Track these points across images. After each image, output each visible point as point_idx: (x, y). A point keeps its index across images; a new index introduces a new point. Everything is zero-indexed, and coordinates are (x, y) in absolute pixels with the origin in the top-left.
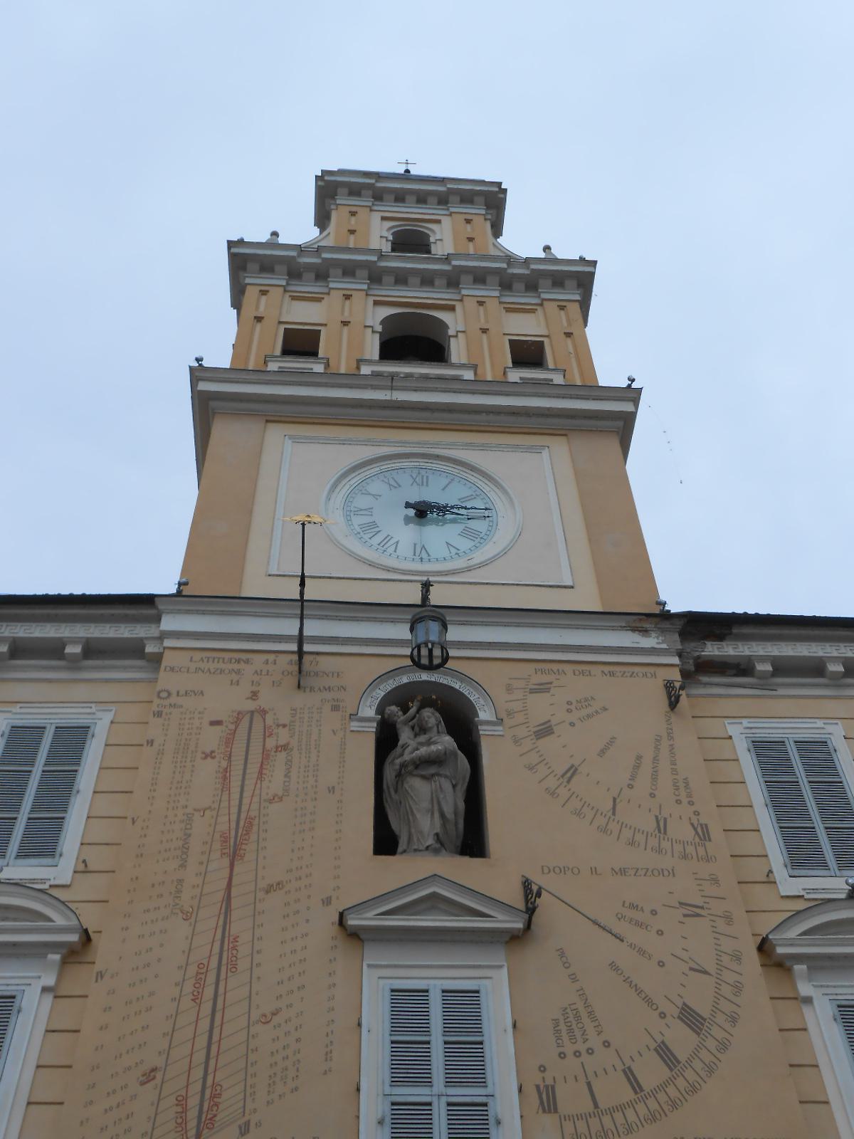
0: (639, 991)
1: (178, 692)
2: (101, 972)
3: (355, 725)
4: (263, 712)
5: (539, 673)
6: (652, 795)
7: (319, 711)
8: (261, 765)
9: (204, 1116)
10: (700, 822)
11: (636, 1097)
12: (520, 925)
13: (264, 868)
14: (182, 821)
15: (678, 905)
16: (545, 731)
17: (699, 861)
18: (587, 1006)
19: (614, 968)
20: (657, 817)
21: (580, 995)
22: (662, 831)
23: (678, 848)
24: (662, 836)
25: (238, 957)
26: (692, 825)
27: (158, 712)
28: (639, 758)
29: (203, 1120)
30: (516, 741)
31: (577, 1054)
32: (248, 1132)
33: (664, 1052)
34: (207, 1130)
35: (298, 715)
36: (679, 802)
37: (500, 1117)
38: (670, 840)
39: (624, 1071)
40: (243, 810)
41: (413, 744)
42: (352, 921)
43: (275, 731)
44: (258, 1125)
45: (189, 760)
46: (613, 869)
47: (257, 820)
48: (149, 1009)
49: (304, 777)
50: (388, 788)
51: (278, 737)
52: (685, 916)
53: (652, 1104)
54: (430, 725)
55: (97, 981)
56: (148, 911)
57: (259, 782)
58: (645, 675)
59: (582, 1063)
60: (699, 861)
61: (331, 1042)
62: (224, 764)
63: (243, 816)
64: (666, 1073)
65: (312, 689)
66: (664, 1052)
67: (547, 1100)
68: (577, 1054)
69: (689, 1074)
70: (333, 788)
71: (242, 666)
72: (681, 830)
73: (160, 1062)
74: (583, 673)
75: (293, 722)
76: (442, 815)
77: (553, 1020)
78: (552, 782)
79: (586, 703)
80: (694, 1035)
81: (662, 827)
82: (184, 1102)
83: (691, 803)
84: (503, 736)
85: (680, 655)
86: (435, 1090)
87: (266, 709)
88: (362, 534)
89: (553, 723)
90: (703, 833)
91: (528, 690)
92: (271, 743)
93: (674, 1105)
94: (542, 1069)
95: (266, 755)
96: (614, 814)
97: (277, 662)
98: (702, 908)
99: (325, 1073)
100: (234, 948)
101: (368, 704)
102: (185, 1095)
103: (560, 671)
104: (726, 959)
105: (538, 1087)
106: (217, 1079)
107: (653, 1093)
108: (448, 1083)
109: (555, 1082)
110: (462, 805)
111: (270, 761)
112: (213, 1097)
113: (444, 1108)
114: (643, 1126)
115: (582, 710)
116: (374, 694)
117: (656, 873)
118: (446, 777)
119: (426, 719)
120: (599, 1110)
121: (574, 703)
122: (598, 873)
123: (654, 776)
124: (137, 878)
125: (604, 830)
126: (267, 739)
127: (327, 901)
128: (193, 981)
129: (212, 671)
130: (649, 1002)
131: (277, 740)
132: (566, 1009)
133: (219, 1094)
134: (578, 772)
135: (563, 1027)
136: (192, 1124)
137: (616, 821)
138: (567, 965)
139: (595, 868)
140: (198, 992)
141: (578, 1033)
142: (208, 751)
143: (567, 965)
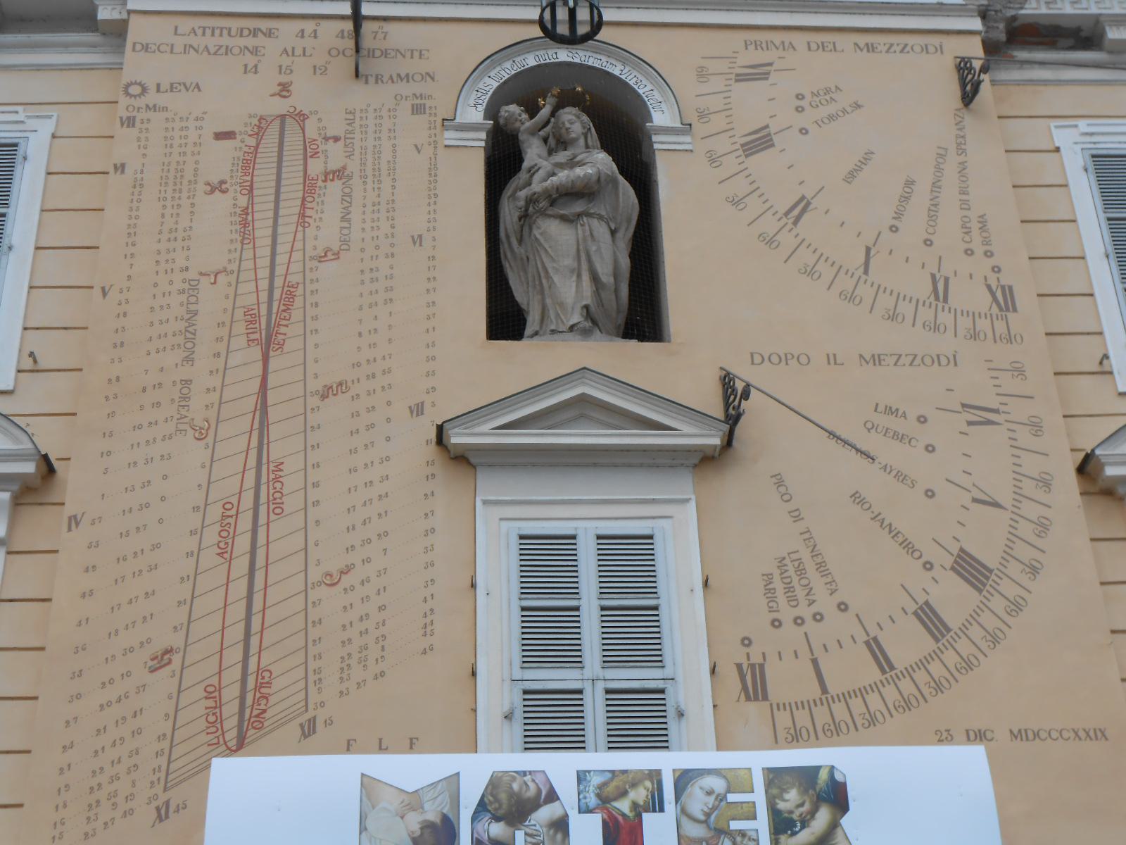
0: (894, 533)
1: (158, 86)
2: (75, 517)
3: (450, 137)
4: (301, 117)
6: (928, 243)
7: (392, 113)
9: (248, 712)
10: (1003, 283)
11: (883, 678)
12: (716, 441)
13: (316, 361)
14: (182, 292)
15: (960, 409)
16: (760, 142)
19: (857, 500)
20: (933, 276)
21: (804, 540)
23: (964, 323)
24: (940, 305)
25: (285, 491)
26: (989, 287)
27: (128, 118)
28: (910, 183)
29: (247, 716)
30: (713, 159)
31: (799, 621)
32: (314, 732)
34: (253, 731)
35: (358, 122)
36: (969, 252)
37: (683, 707)
38: (953, 311)
39: (867, 643)
40: (277, 273)
41: (546, 165)
42: (457, 438)
43: (322, 148)
45: (184, 195)
46: (861, 356)
47: (301, 287)
48: (153, 568)
49: (373, 221)
50: (508, 237)
51: (327, 157)
52: (970, 423)
53: (906, 686)
54: (573, 135)
55: (70, 530)
56: (140, 427)
57: (300, 228)
58: (925, 49)
59: (806, 633)
61: (432, 610)
62: (243, 201)
63: (278, 282)
64: (928, 644)
65: (378, 79)
67: (754, 685)
68: (799, 621)
69: (963, 646)
70: (420, 237)
71: (261, 40)
72: (970, 296)
73: (177, 641)
74: (823, 47)
76: (595, 278)
77: (763, 575)
80: (976, 593)
81: (940, 291)
82: (216, 694)
83: (989, 254)
84: (691, 151)
85: (984, 15)
86: (588, 673)
87: (306, 112)
89: (772, 130)
90: (1005, 300)
91: (733, 76)
92: (316, 167)
94: (746, 642)
95: (309, 187)
96: (866, 272)
97: (318, 33)
98: (996, 411)
99: (424, 652)
100: (277, 480)
101: (472, 102)
102: (217, 685)
103: (786, 44)
104: (1028, 487)
105: (739, 666)
107: (909, 672)
108: (607, 663)
109: (764, 659)
110: (625, 262)
111: (316, 196)
112: (258, 687)
113: (600, 697)
114: (892, 716)
116: (481, 85)
117: (928, 360)
118: (600, 217)
119: (567, 125)
120: (829, 696)
121: (808, 98)
122: (838, 362)
123: (932, 213)
124: (118, 379)
126: (310, 161)
127: (418, 410)
128: (217, 528)
129: (212, 50)
130: (908, 546)
131: (326, 163)
132: (784, 558)
133: (267, 683)
134: (811, 207)
135: (778, 585)
136: (231, 723)
137: (869, 283)
138: (786, 497)
139: (835, 355)
140: (227, 543)
141: (800, 593)
142: (215, 180)
143: (787, 498)
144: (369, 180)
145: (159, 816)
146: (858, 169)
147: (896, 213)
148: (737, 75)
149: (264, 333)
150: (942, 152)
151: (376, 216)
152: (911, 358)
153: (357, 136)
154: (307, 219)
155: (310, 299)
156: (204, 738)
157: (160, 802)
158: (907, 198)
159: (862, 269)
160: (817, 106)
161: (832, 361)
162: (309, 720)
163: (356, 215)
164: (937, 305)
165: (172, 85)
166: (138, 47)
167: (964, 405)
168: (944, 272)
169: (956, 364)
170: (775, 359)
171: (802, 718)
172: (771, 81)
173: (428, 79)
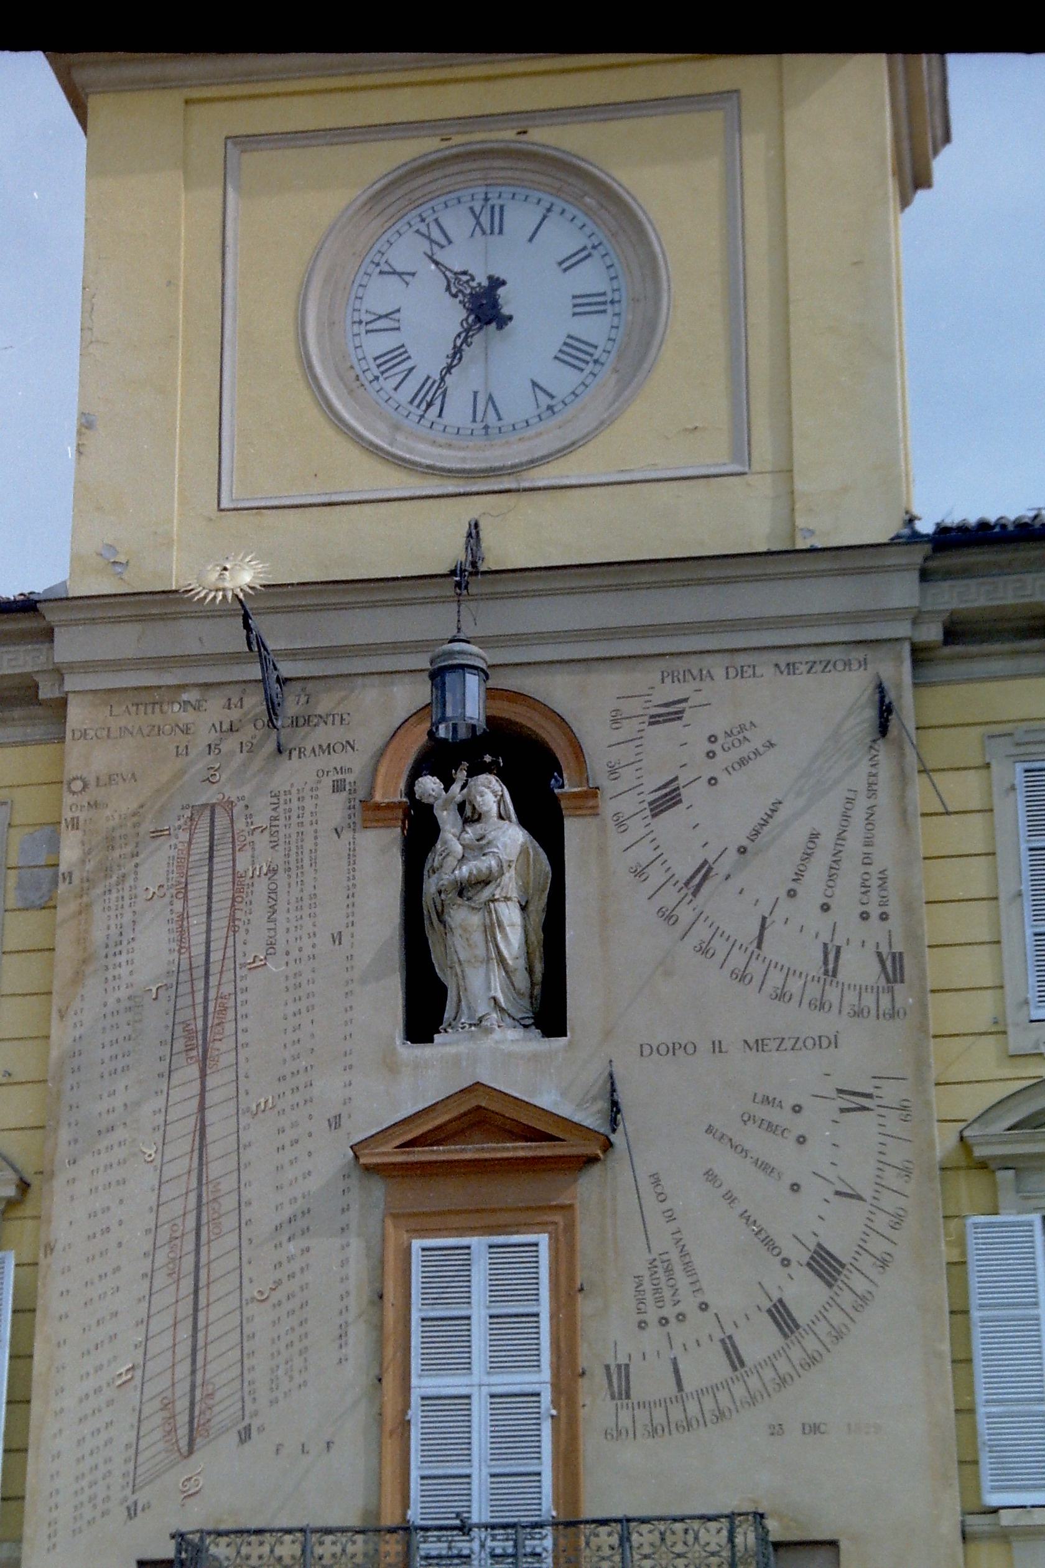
5: (668, 680)
6: (825, 908)
8: (233, 905)
15: (834, 1094)
16: (668, 799)
18: (683, 1253)
20: (825, 945)
26: (879, 955)
27: (73, 819)
28: (814, 836)
31: (664, 1321)
33: (781, 1316)
35: (282, 807)
39: (722, 1341)
44: (261, 1429)
46: (746, 1042)
52: (842, 1110)
60: (878, 1017)
63: (212, 994)
66: (781, 1316)
68: (664, 1321)
75: (276, 819)
78: (669, 897)
79: (740, 737)
86: (475, 1379)
88: (381, 379)
89: (681, 782)
91: (646, 719)
93: (783, 1381)
96: (759, 947)
98: (869, 1096)
106: (208, 1376)
108: (495, 1367)
115: (733, 749)
117: (809, 1043)
123: (834, 871)
125: (741, 977)
135: (647, 1285)
136: (183, 1431)
138: (662, 1197)
139: (720, 1042)
141: (667, 1293)
144: (293, 873)
145: (129, 1514)
148: (652, 717)
149: (200, 1050)
150: (851, 795)
151: (299, 913)
152: (793, 1041)
153: (282, 822)
154: (237, 923)
155: (241, 1011)
156: (161, 1446)
157: (130, 1502)
159: (755, 944)
161: (717, 1050)
162: (245, 1428)
163: (280, 917)
165: (110, 776)
166: (78, 734)
167: (840, 1091)
170: (663, 1050)
171: (659, 1415)
172: (685, 721)
173: (349, 748)
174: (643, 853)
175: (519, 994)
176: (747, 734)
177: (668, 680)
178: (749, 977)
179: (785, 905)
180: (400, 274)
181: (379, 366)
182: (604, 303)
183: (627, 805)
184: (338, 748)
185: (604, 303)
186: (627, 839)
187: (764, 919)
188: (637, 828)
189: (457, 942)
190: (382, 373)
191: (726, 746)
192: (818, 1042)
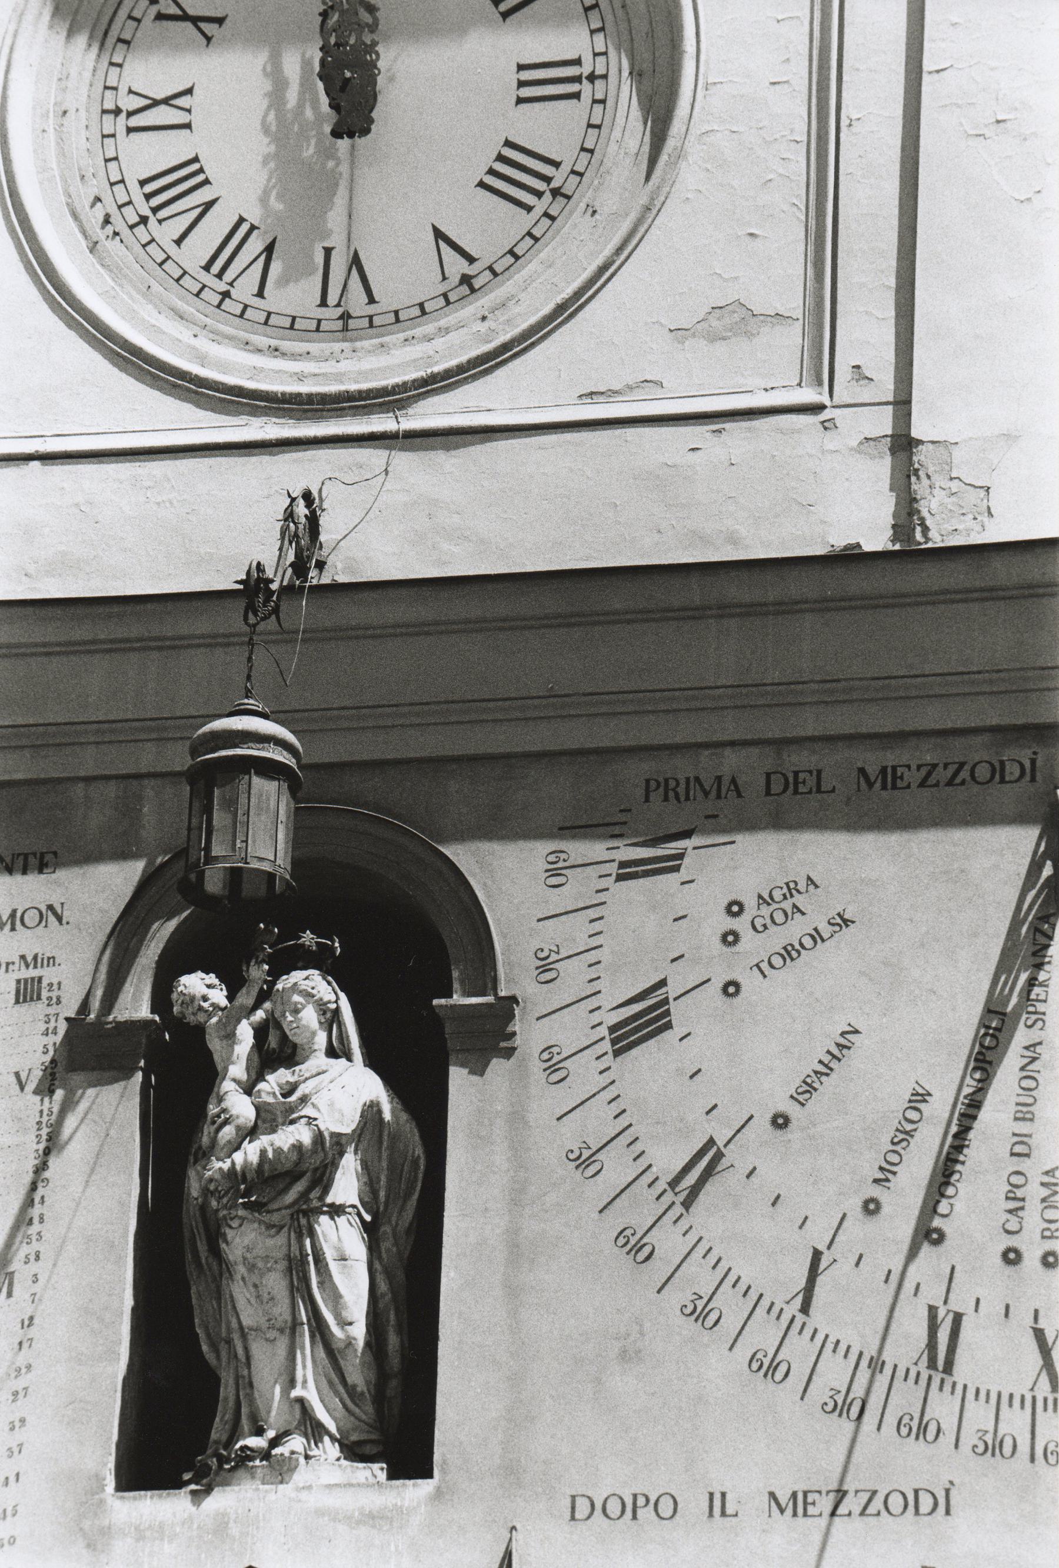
5: (656, 797)
16: (645, 1022)
17: (1032, 1459)
20: (932, 1310)
22: (940, 1367)
28: (919, 1097)
46: (772, 1495)
60: (1032, 1459)
79: (787, 905)
88: (152, 221)
89: (673, 990)
96: (805, 1309)
115: (773, 929)
134: (724, 1162)
137: (808, 1332)
139: (723, 1495)
146: (825, 1070)
147: (881, 1169)
148: (623, 865)
152: (864, 1497)
158: (907, 1133)
159: (798, 1301)
160: (765, 926)
161: (717, 1510)
164: (930, 1378)
168: (961, 1301)
169: (948, 1512)
170: (614, 1507)
172: (683, 874)
173: (52, 919)
174: (597, 1123)
175: (351, 1391)
176: (799, 900)
177: (656, 797)
178: (783, 1368)
179: (857, 1228)
180: (195, 20)
181: (148, 197)
182: (577, 79)
183: (569, 1031)
184: (32, 918)
185: (577, 79)
186: (565, 1097)
187: (817, 1255)
188: (585, 1074)
189: (240, 1293)
190: (155, 210)
191: (758, 923)
192: (912, 1503)
